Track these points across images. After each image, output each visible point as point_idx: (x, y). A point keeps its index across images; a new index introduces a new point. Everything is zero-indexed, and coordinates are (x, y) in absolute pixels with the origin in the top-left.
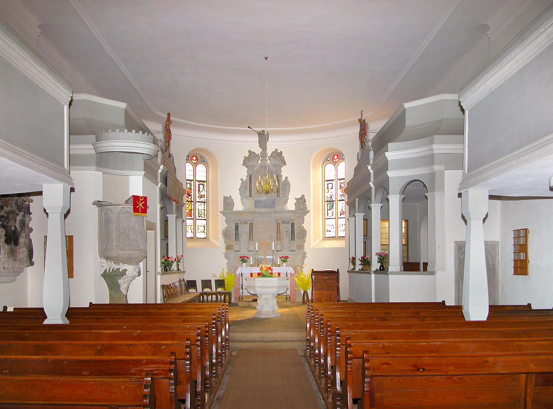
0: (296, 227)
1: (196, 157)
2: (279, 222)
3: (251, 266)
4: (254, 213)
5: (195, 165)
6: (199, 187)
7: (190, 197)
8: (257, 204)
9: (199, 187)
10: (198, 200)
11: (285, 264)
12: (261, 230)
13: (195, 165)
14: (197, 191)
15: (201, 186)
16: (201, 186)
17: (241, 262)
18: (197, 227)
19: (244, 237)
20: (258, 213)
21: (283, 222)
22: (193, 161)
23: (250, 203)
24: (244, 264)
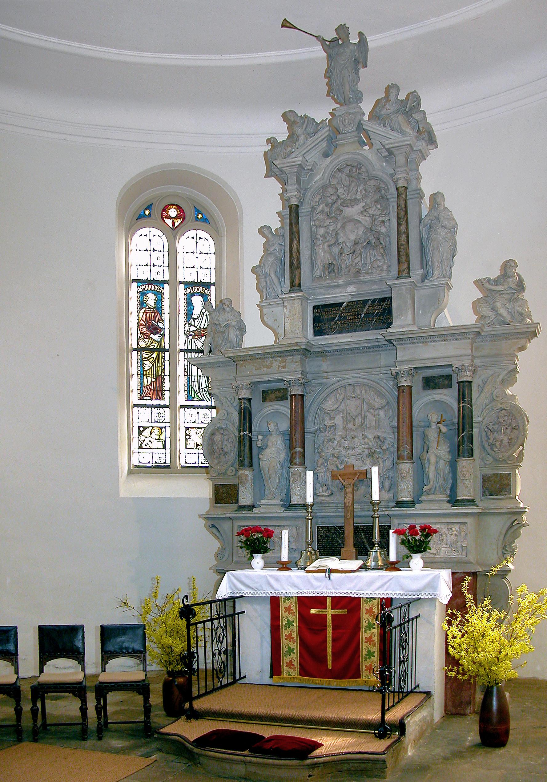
0: (479, 400)
1: (178, 207)
2: (404, 382)
3: (285, 567)
4: (306, 352)
5: (173, 234)
6: (189, 304)
7: (156, 337)
8: (326, 318)
9: (189, 304)
10: (182, 343)
11: (417, 560)
12: (339, 420)
13: (173, 234)
14: (182, 319)
15: (197, 301)
16: (197, 301)
17: (245, 553)
18: (181, 434)
19: (273, 453)
20: (323, 354)
21: (430, 383)
22: (169, 222)
23: (296, 323)
24: (258, 560)
